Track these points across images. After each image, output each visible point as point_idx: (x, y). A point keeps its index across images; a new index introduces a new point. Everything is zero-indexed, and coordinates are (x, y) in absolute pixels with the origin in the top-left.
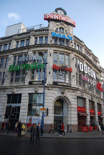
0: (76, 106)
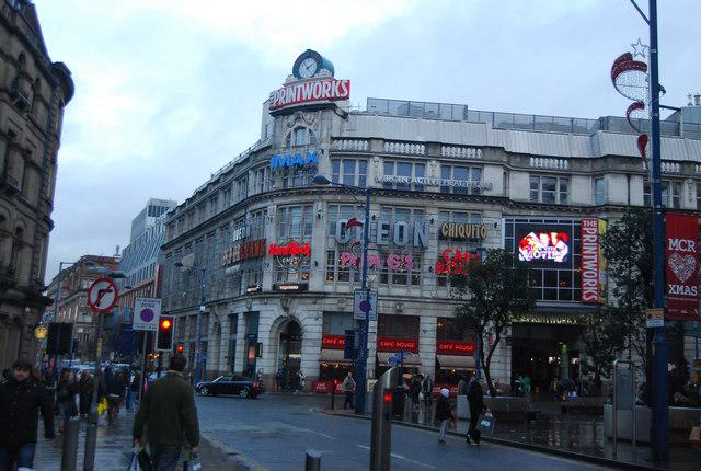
0: (319, 336)
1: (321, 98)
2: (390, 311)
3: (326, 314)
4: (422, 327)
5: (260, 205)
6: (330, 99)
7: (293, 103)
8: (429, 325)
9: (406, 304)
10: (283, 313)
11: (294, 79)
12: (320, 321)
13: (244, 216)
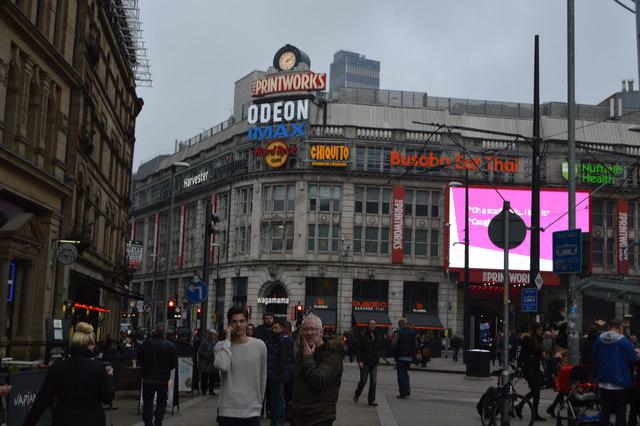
1: (300, 89)
2: (363, 277)
3: (309, 280)
4: (391, 290)
5: (245, 183)
6: (309, 90)
7: (274, 92)
8: (396, 288)
9: (377, 271)
10: (270, 278)
11: (275, 71)
12: (304, 286)
13: (230, 191)
